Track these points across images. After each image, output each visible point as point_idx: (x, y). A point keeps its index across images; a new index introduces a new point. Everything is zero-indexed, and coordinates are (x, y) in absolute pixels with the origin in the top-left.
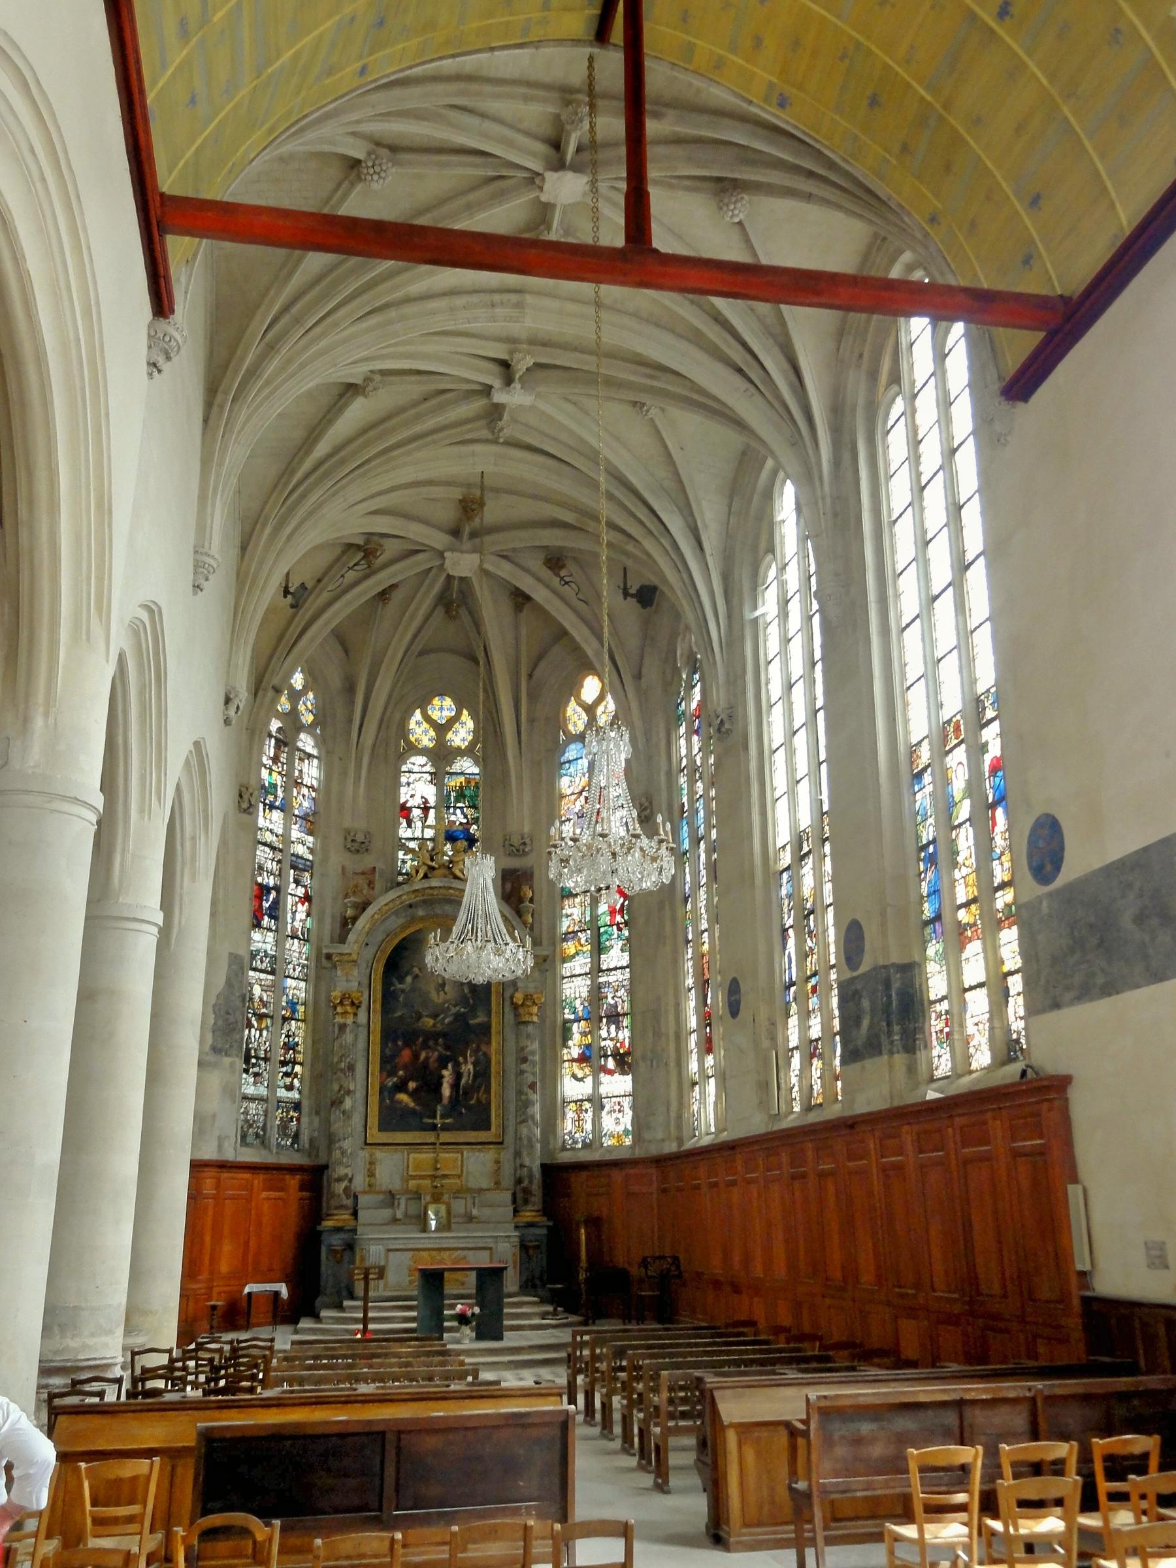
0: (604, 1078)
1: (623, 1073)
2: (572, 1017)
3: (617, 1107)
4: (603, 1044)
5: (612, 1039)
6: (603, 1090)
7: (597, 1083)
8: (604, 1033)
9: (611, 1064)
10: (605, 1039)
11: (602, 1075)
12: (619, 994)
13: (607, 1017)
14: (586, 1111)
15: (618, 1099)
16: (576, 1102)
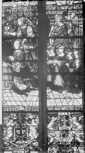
0: (51, 94)
1: (73, 90)
2: (14, 34)
3: (65, 121)
4: (50, 62)
5: (60, 59)
6: (50, 103)
7: (43, 98)
8: (51, 53)
9: (59, 81)
10: (52, 58)
11: (48, 90)
12: (69, 18)
13: (55, 38)
14: (30, 120)
15: (66, 114)
16: (17, 113)
